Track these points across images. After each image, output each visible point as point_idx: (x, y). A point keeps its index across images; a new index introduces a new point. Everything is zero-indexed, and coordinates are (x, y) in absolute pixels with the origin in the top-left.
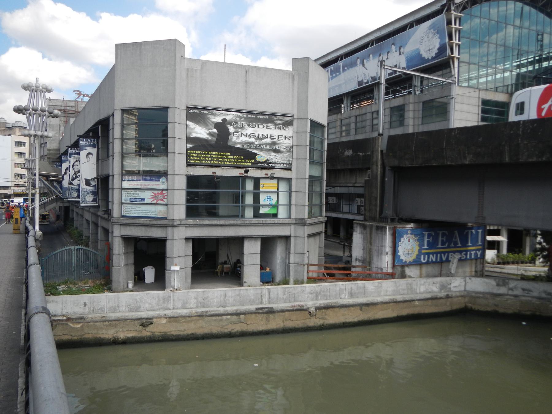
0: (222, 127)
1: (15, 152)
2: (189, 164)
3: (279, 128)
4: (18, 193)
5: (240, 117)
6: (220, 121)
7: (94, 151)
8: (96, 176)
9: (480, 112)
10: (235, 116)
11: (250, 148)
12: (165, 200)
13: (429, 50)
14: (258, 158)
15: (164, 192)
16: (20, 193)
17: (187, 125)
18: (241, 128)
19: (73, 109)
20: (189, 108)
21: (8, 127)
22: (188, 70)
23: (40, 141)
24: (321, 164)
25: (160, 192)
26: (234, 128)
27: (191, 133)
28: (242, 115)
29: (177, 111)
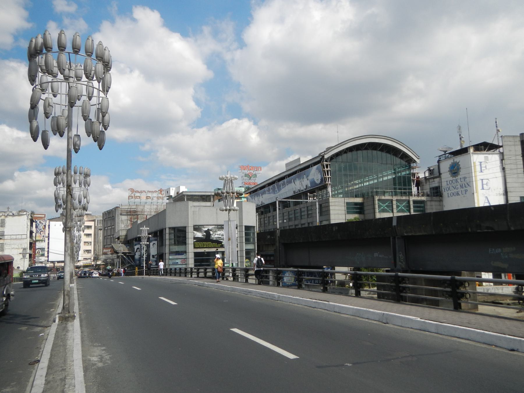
0: (208, 232)
2: (195, 247)
4: (86, 264)
5: (215, 227)
6: (207, 230)
7: (156, 242)
8: (156, 253)
9: (346, 209)
11: (220, 240)
13: (318, 180)
16: (87, 264)
17: (194, 233)
18: (215, 232)
19: (135, 210)
20: (194, 226)
22: (193, 211)
23: (104, 225)
24: (254, 243)
25: (184, 259)
26: (213, 232)
27: (195, 236)
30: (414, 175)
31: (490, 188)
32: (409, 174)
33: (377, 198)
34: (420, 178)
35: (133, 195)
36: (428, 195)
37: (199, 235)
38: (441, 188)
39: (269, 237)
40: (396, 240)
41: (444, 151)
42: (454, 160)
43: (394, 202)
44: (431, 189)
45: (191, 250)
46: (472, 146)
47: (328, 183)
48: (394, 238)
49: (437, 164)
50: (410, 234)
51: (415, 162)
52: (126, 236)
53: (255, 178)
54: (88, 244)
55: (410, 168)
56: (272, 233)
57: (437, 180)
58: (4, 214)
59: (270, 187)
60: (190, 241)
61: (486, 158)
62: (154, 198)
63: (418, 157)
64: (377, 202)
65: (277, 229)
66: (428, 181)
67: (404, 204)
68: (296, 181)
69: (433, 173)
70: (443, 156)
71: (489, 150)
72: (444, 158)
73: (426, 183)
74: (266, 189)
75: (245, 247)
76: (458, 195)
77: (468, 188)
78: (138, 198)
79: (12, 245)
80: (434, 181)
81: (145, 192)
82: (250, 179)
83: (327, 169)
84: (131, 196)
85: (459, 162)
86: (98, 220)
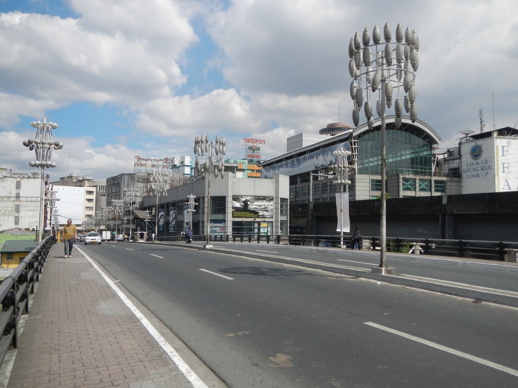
0: (246, 202)
1: (86, 199)
2: (233, 217)
3: (267, 202)
5: (252, 198)
9: (370, 186)
10: (251, 198)
11: (256, 210)
12: (224, 231)
14: (259, 214)
15: (224, 228)
17: (232, 202)
18: (252, 202)
21: (79, 179)
23: (108, 191)
24: (287, 215)
25: (222, 228)
26: (250, 202)
27: (234, 205)
28: (253, 198)
29: (229, 197)
30: (434, 155)
31: (510, 172)
32: (430, 154)
33: (401, 177)
34: (439, 158)
35: (139, 163)
36: (447, 176)
37: (238, 205)
38: (460, 170)
39: (301, 209)
40: (447, 218)
41: (465, 134)
42: (476, 143)
43: (417, 181)
44: (449, 170)
45: (230, 219)
46: (496, 130)
47: (355, 160)
48: (444, 216)
49: (458, 146)
50: (461, 213)
51: (436, 143)
52: (142, 203)
53: (258, 151)
54: (90, 209)
55: (431, 149)
56: (305, 206)
57: (457, 161)
58: (19, 176)
59: (289, 162)
60: (229, 210)
61: (509, 143)
62: (159, 167)
63: (439, 139)
64: (401, 180)
65: (310, 202)
66: (447, 163)
67: (426, 183)
68: (319, 156)
69: (452, 155)
70: (465, 139)
71: (512, 134)
72: (465, 141)
73: (445, 164)
74: (283, 163)
75: (281, 218)
76: (478, 177)
77: (489, 171)
78: (144, 166)
79: (28, 207)
80: (453, 163)
81: (151, 161)
82: (253, 152)
83: (355, 146)
84: (137, 164)
85: (481, 146)
86: (100, 186)
